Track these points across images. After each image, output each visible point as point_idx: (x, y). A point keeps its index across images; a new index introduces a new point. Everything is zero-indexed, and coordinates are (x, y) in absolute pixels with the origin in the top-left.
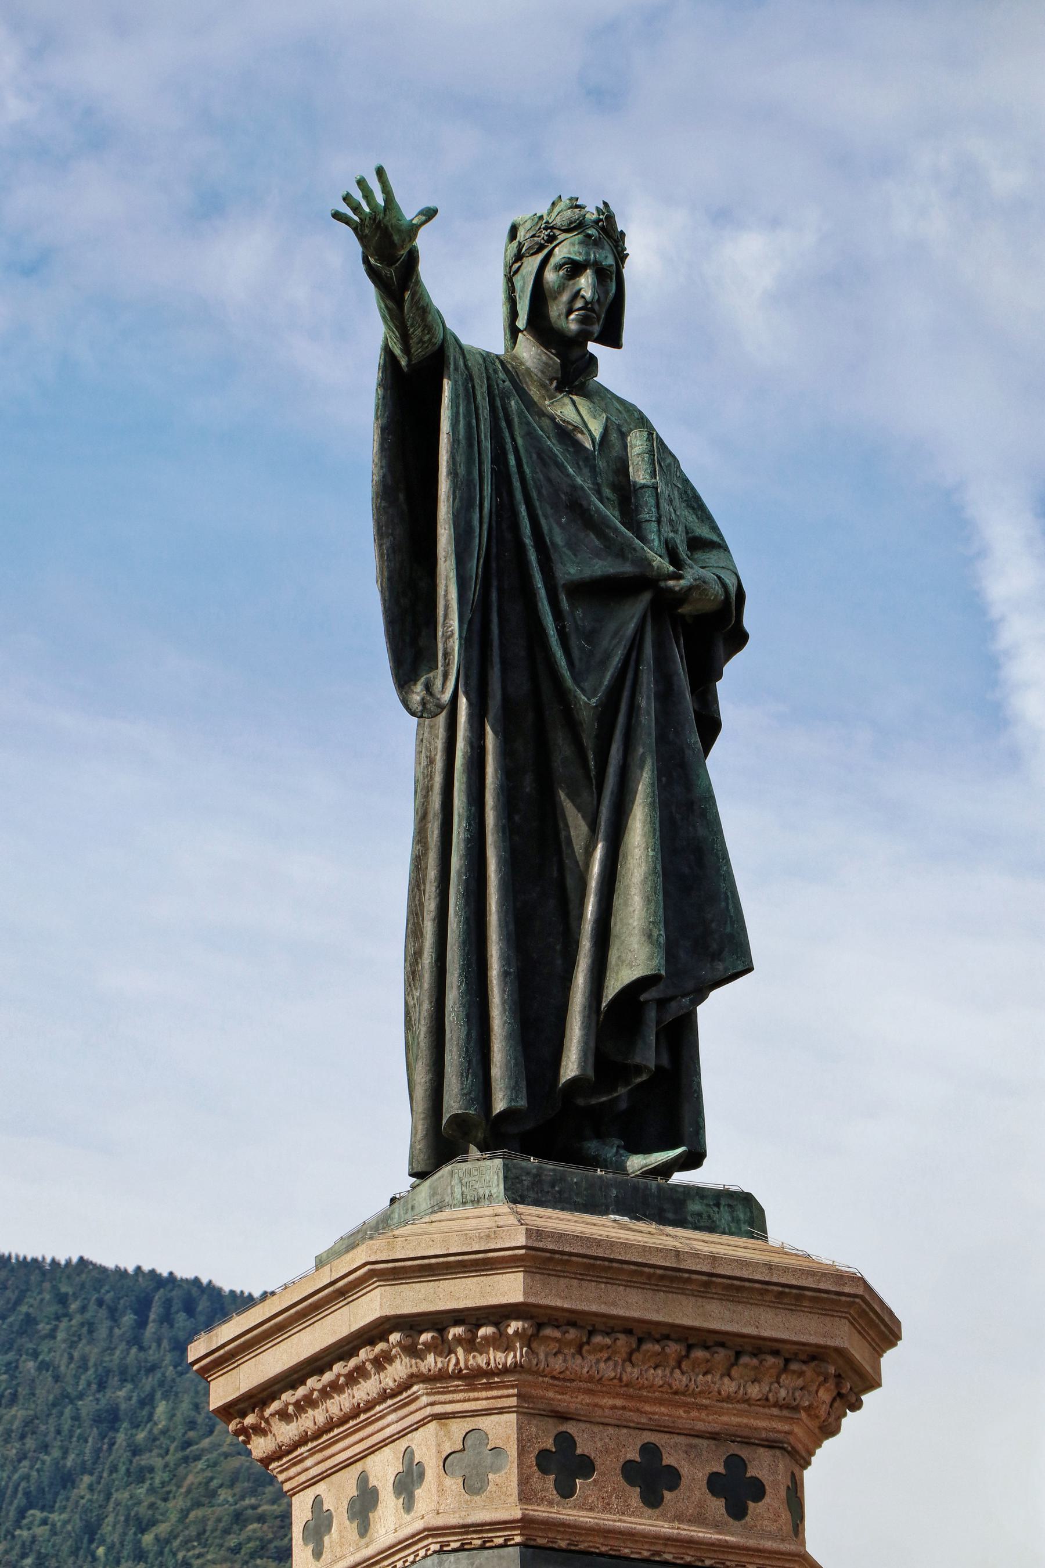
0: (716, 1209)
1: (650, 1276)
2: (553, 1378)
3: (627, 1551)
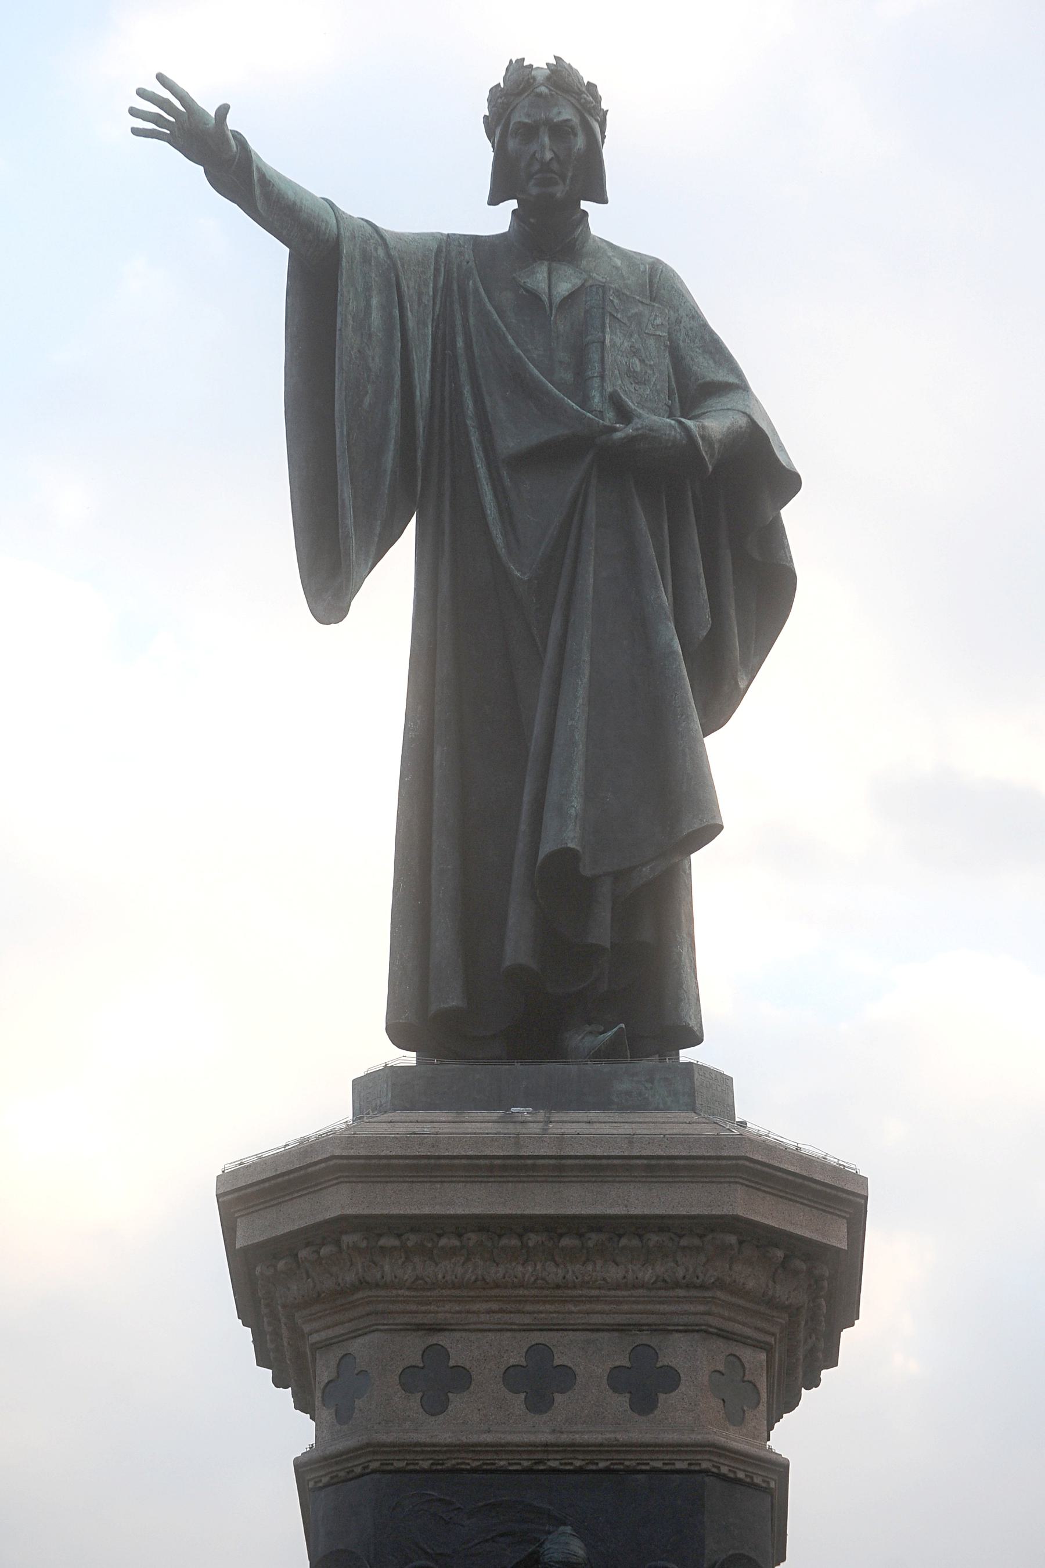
0: (649, 1085)
1: (491, 1168)
2: (409, 1289)
3: (502, 1463)
